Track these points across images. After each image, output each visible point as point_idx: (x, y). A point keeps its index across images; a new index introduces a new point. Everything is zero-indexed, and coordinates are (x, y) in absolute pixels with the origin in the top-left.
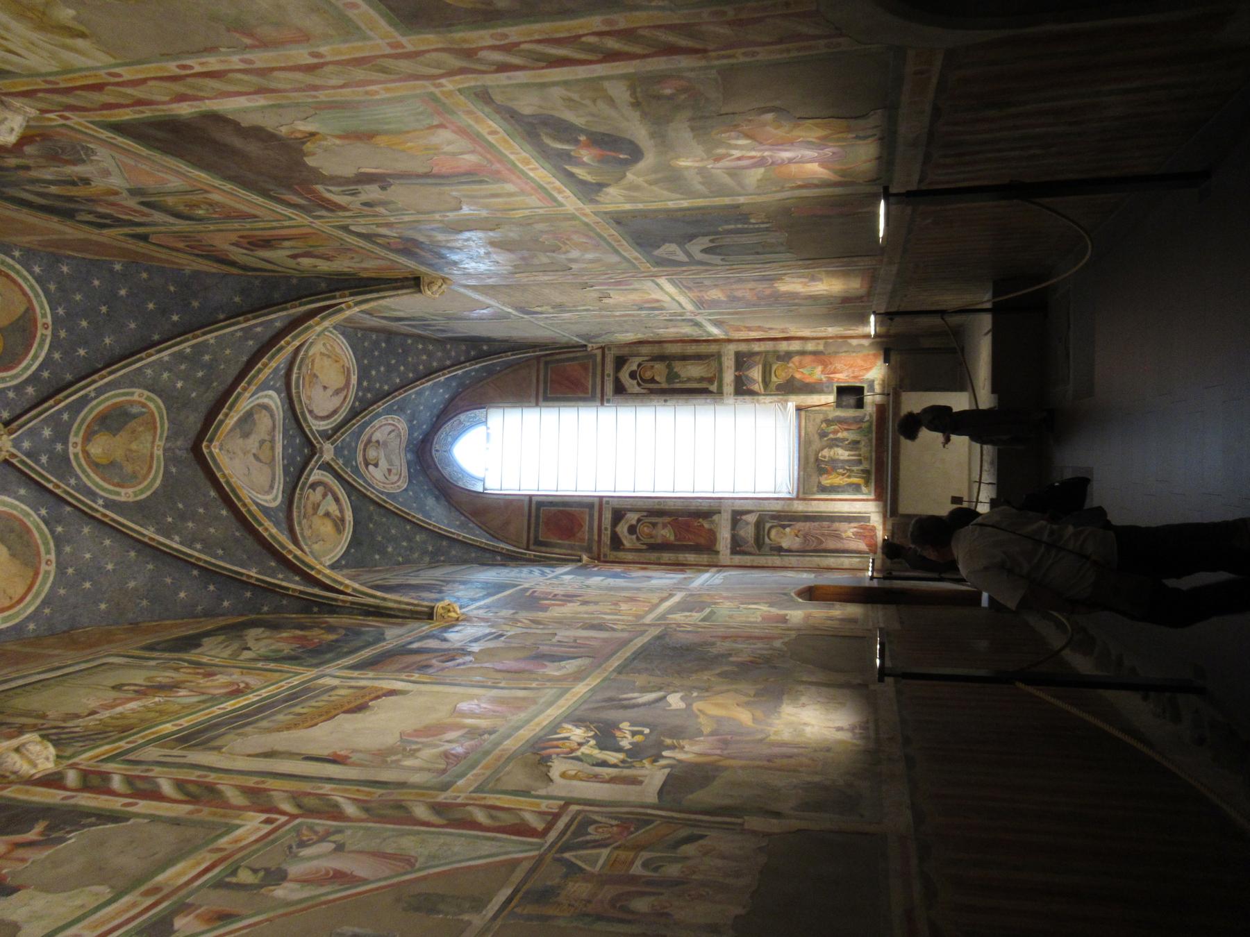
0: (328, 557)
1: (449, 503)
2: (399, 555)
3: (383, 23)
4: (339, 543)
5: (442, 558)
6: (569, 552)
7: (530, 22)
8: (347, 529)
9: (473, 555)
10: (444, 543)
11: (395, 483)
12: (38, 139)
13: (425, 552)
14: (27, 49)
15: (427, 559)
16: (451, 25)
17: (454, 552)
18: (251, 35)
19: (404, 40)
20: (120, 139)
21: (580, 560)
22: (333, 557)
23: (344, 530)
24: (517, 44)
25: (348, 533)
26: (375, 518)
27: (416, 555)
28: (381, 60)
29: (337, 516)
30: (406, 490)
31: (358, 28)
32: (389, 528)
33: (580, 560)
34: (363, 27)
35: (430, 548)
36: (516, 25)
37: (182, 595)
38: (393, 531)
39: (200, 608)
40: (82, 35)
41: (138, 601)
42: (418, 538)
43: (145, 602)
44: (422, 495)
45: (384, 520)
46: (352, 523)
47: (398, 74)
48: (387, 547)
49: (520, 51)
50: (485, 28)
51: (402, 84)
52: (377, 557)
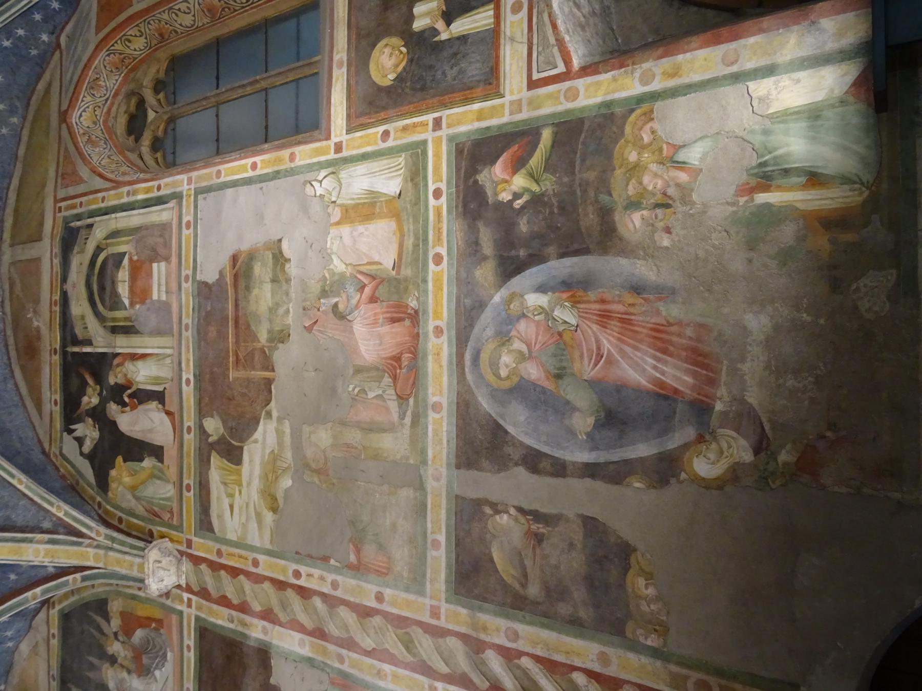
3: (443, 576)
7: (544, 626)
12: (154, 625)
14: (241, 509)
16: (485, 600)
18: (358, 551)
19: (444, 607)
20: (192, 655)
24: (521, 654)
28: (414, 627)
31: (424, 576)
34: (428, 575)
36: (530, 623)
40: (274, 510)
47: (414, 655)
49: (519, 667)
50: (507, 617)
51: (406, 672)
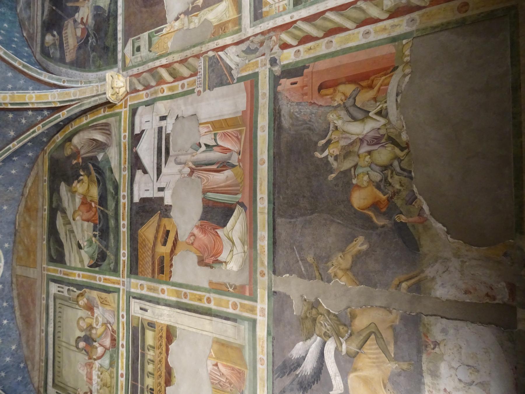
37: (13, 172)
39: (27, 166)
41: (8, 191)
43: (11, 188)
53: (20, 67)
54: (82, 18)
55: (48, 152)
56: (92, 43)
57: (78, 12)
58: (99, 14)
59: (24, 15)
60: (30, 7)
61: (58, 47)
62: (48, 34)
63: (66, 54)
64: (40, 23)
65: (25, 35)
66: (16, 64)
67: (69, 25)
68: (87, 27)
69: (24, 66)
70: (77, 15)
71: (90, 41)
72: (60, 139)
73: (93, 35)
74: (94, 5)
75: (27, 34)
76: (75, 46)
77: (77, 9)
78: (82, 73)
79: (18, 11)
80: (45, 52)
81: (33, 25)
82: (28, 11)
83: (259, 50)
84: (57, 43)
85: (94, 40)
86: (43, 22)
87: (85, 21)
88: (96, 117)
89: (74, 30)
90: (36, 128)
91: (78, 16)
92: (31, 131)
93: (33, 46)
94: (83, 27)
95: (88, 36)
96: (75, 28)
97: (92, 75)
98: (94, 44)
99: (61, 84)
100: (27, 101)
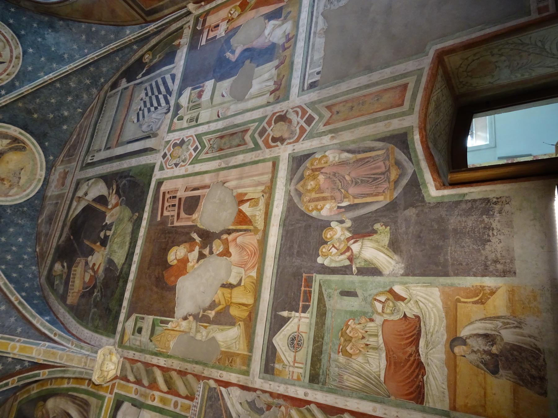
0: (39, 169)
1: (62, 19)
2: (75, 109)
4: (33, 153)
5: (102, 80)
6: (176, 7)
8: (26, 140)
9: (117, 59)
10: (92, 69)
11: (12, 57)
13: (88, 88)
15: (94, 91)
17: (104, 70)
21: (189, 13)
22: (41, 165)
23: (24, 143)
25: (29, 140)
26: (31, 107)
27: (85, 96)
29: (9, 144)
30: (25, 52)
32: (48, 102)
33: (189, 13)
35: (88, 82)
38: (53, 101)
42: (72, 85)
44: (39, 40)
45: (38, 100)
46: (23, 132)
48: (62, 114)
52: (65, 127)
53: (16, 303)
54: (94, 264)
55: (19, 400)
56: (96, 296)
57: (92, 255)
58: (111, 270)
59: (43, 229)
60: (51, 224)
61: (63, 281)
62: (59, 262)
63: (69, 294)
64: (55, 244)
65: (37, 250)
66: (13, 299)
67: (81, 264)
68: (96, 276)
69: (20, 303)
70: (90, 258)
71: (95, 294)
72: (35, 391)
73: (99, 288)
74: (108, 256)
75: (40, 250)
76: (79, 291)
77: (91, 252)
78: (78, 325)
79: (39, 221)
80: (50, 279)
81: (48, 244)
82: (48, 226)
83: (265, 413)
84: (64, 276)
85: (99, 294)
86: (58, 247)
87: (96, 268)
88: (78, 386)
89: (83, 272)
90: (10, 380)
91: (91, 260)
92: (4, 382)
93: (41, 266)
94: (93, 274)
95: (95, 287)
96: (85, 271)
97: (87, 333)
98: (98, 299)
99: (52, 336)
100: (9, 351)
